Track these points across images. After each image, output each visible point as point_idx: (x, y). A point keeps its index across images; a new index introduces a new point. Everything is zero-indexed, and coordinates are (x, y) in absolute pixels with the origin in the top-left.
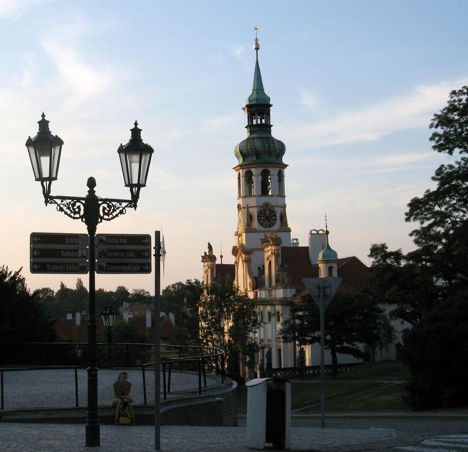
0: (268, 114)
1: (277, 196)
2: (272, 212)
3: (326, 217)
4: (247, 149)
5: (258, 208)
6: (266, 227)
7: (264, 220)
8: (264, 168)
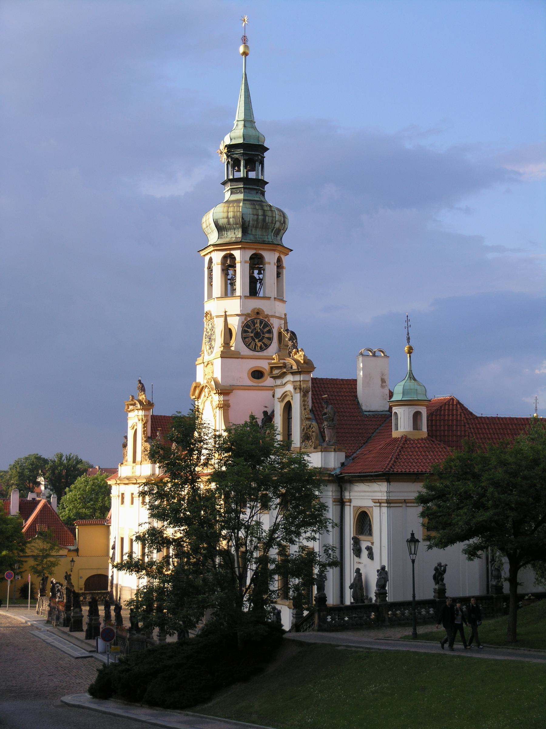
0: (262, 163)
1: (275, 298)
2: (266, 325)
3: (408, 321)
4: (227, 217)
5: (244, 317)
6: (255, 350)
7: (252, 337)
8: (253, 252)
